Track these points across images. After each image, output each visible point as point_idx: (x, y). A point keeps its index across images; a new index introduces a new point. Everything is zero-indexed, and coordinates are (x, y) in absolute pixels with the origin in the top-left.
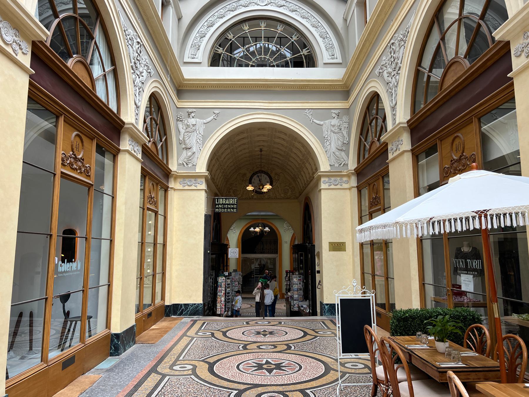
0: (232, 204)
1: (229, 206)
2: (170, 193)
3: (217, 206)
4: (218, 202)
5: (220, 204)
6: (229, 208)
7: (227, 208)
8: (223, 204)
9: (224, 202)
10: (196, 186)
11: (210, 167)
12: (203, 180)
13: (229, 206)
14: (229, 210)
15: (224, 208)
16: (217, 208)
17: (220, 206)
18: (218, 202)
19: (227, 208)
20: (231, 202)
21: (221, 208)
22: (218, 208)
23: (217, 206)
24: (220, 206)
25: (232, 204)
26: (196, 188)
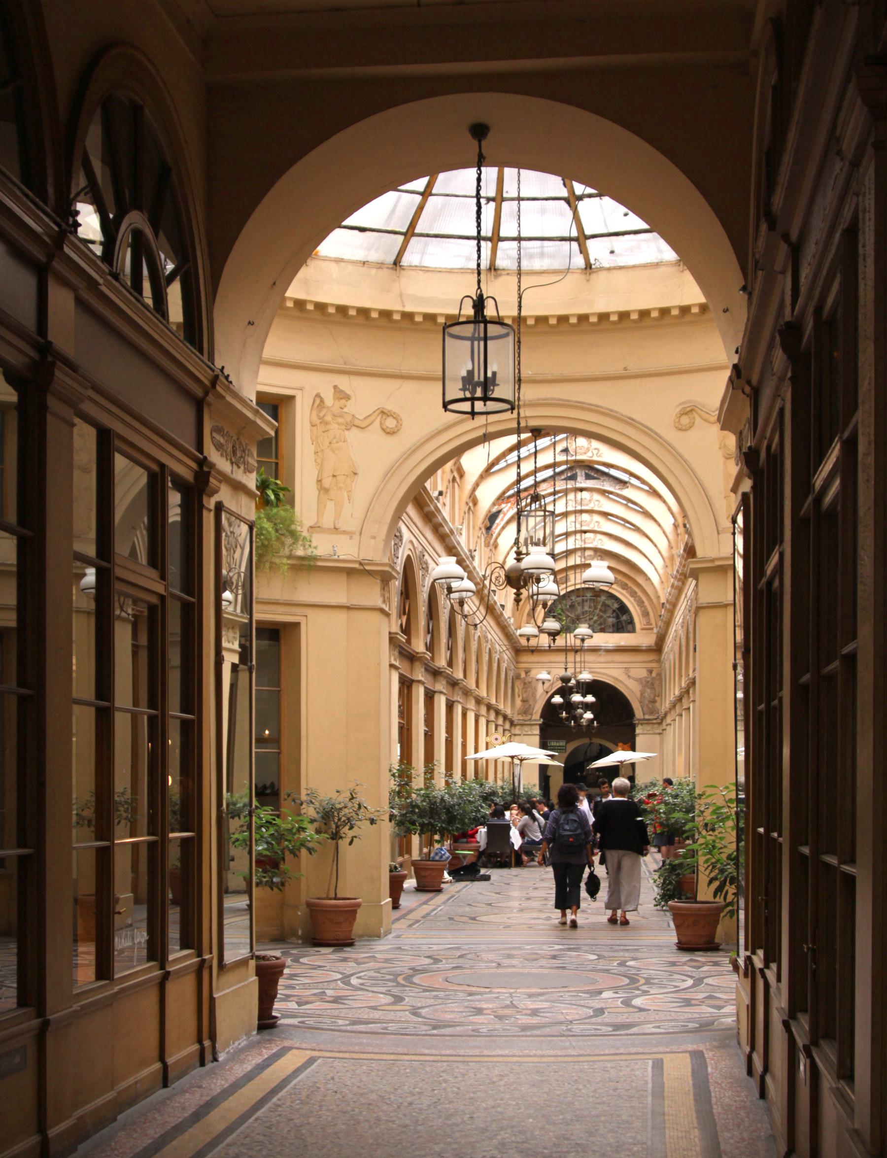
11: (542, 716)
12: (538, 727)
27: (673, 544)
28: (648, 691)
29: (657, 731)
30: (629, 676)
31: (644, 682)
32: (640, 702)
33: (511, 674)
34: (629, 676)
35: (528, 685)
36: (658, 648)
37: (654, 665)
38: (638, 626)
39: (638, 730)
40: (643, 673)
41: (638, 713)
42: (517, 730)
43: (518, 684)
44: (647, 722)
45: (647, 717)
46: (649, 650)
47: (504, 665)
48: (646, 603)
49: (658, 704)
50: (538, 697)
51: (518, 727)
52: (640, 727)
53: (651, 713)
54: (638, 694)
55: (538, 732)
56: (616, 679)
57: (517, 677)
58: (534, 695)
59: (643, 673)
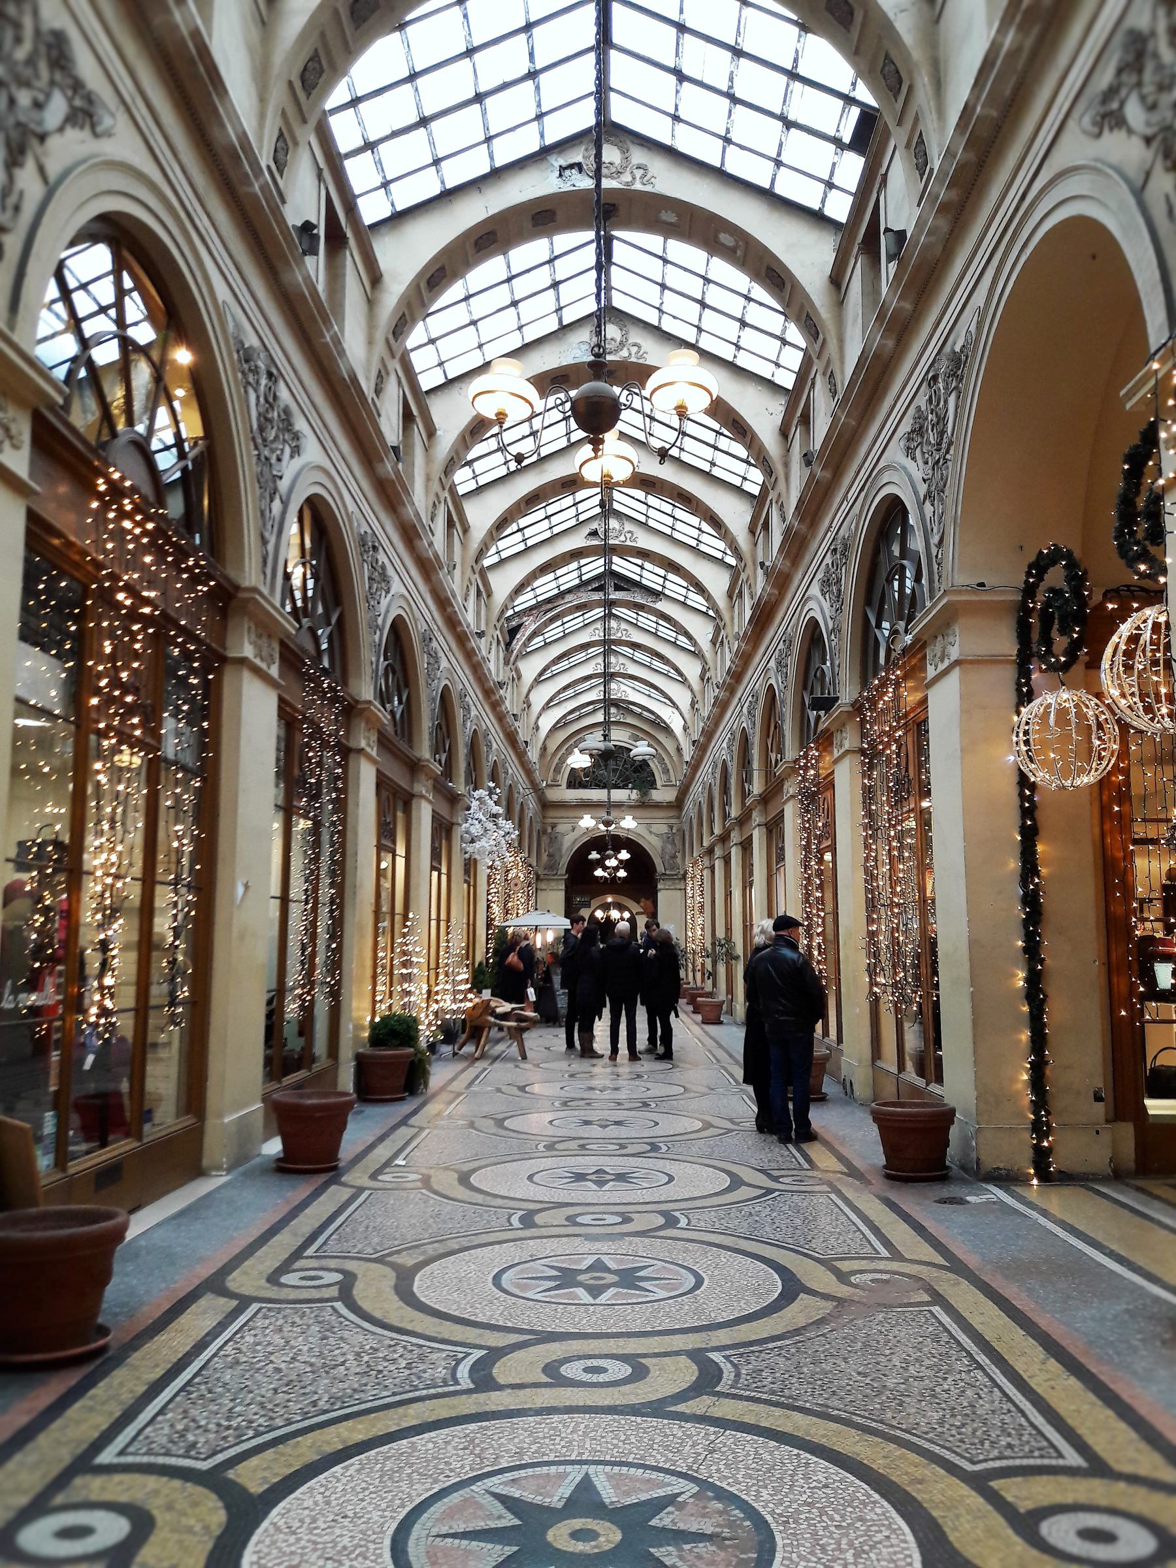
27: (699, 698)
28: (670, 846)
33: (537, 827)
35: (554, 839)
36: (678, 805)
37: (673, 821)
38: (659, 783)
40: (664, 829)
41: (660, 868)
42: (542, 885)
43: (545, 839)
46: (669, 806)
47: (529, 813)
48: (667, 761)
49: (679, 860)
53: (672, 869)
57: (544, 832)
59: (664, 829)
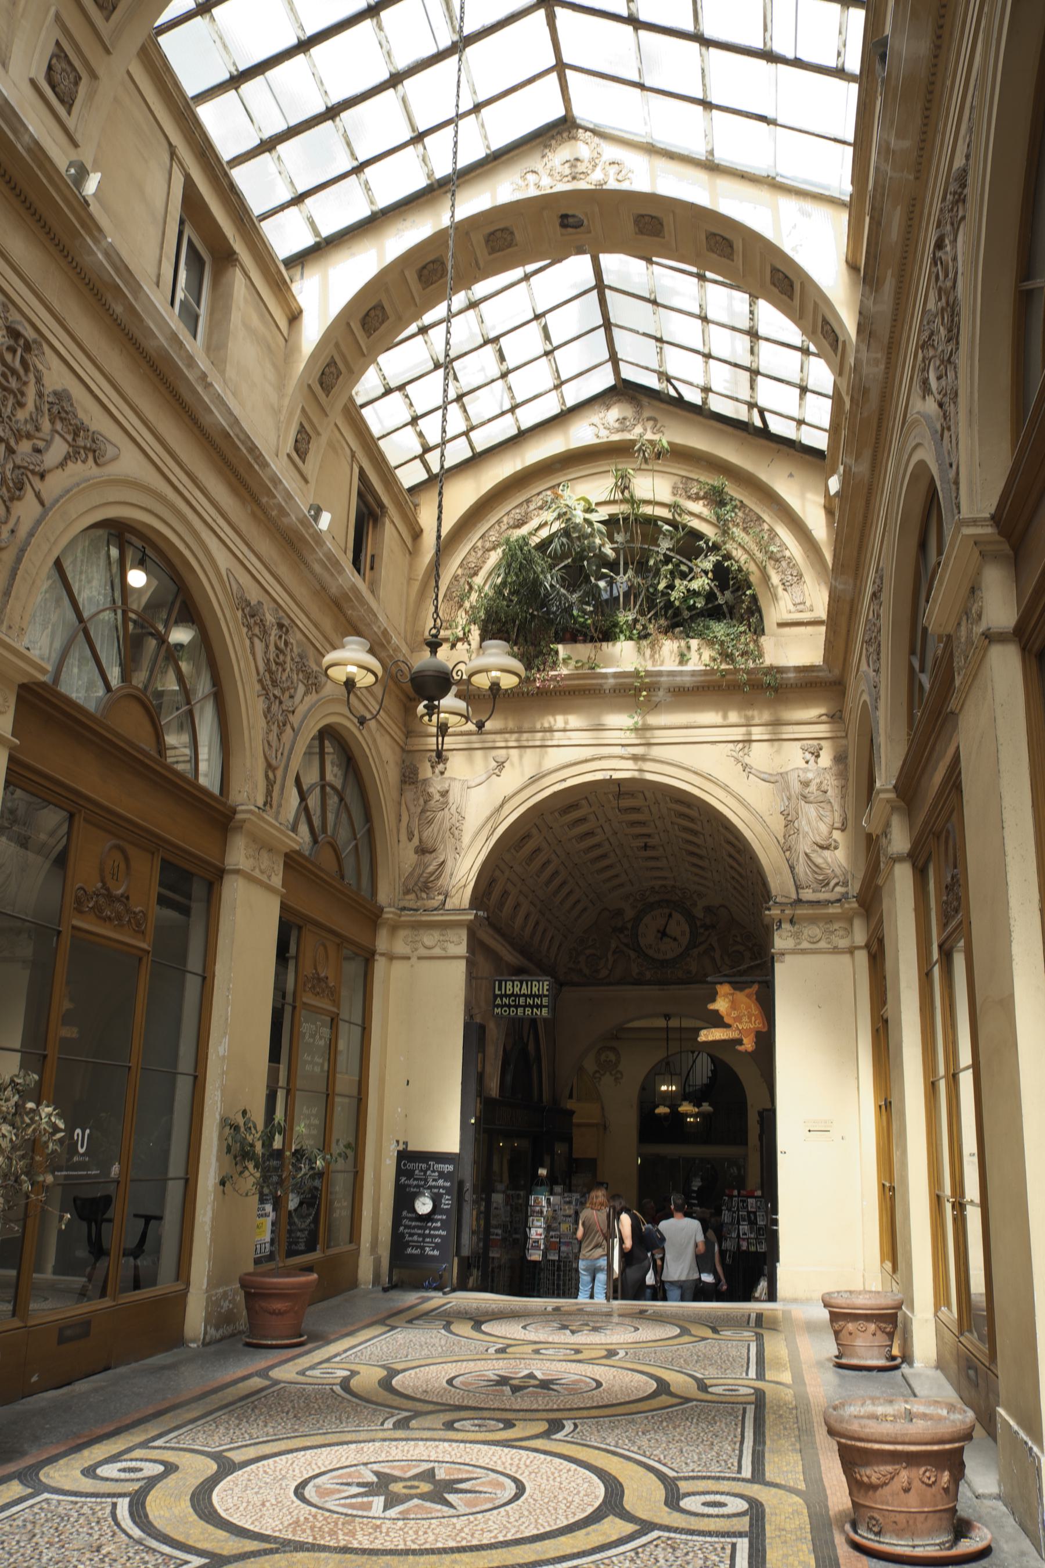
0: (538, 996)
1: (530, 1001)
2: (380, 965)
3: (498, 1001)
4: (500, 989)
5: (506, 996)
6: (530, 1006)
7: (525, 1007)
8: (512, 995)
9: (517, 990)
10: (444, 949)
13: (530, 1001)
14: (528, 1011)
15: (517, 1007)
16: (498, 1006)
17: (506, 1001)
18: (500, 989)
19: (525, 1007)
20: (535, 989)
21: (509, 1006)
22: (502, 1006)
23: (498, 1001)
24: (506, 1001)
25: (538, 996)
26: (442, 953)
29: (843, 943)
30: (745, 767)
31: (796, 787)
32: (787, 849)
34: (745, 767)
39: (781, 941)
41: (779, 883)
44: (803, 910)
45: (807, 895)
50: (466, 839)
51: (402, 933)
52: (786, 926)
54: (777, 824)
55: (462, 949)
56: (708, 778)
58: (454, 831)
